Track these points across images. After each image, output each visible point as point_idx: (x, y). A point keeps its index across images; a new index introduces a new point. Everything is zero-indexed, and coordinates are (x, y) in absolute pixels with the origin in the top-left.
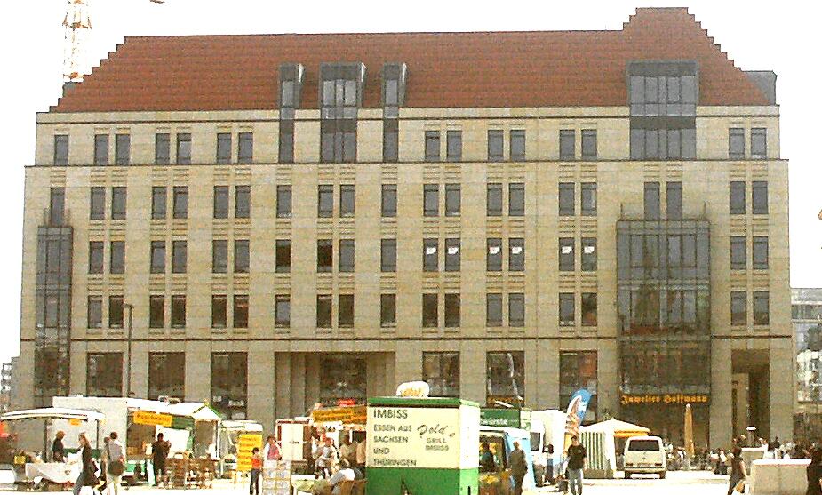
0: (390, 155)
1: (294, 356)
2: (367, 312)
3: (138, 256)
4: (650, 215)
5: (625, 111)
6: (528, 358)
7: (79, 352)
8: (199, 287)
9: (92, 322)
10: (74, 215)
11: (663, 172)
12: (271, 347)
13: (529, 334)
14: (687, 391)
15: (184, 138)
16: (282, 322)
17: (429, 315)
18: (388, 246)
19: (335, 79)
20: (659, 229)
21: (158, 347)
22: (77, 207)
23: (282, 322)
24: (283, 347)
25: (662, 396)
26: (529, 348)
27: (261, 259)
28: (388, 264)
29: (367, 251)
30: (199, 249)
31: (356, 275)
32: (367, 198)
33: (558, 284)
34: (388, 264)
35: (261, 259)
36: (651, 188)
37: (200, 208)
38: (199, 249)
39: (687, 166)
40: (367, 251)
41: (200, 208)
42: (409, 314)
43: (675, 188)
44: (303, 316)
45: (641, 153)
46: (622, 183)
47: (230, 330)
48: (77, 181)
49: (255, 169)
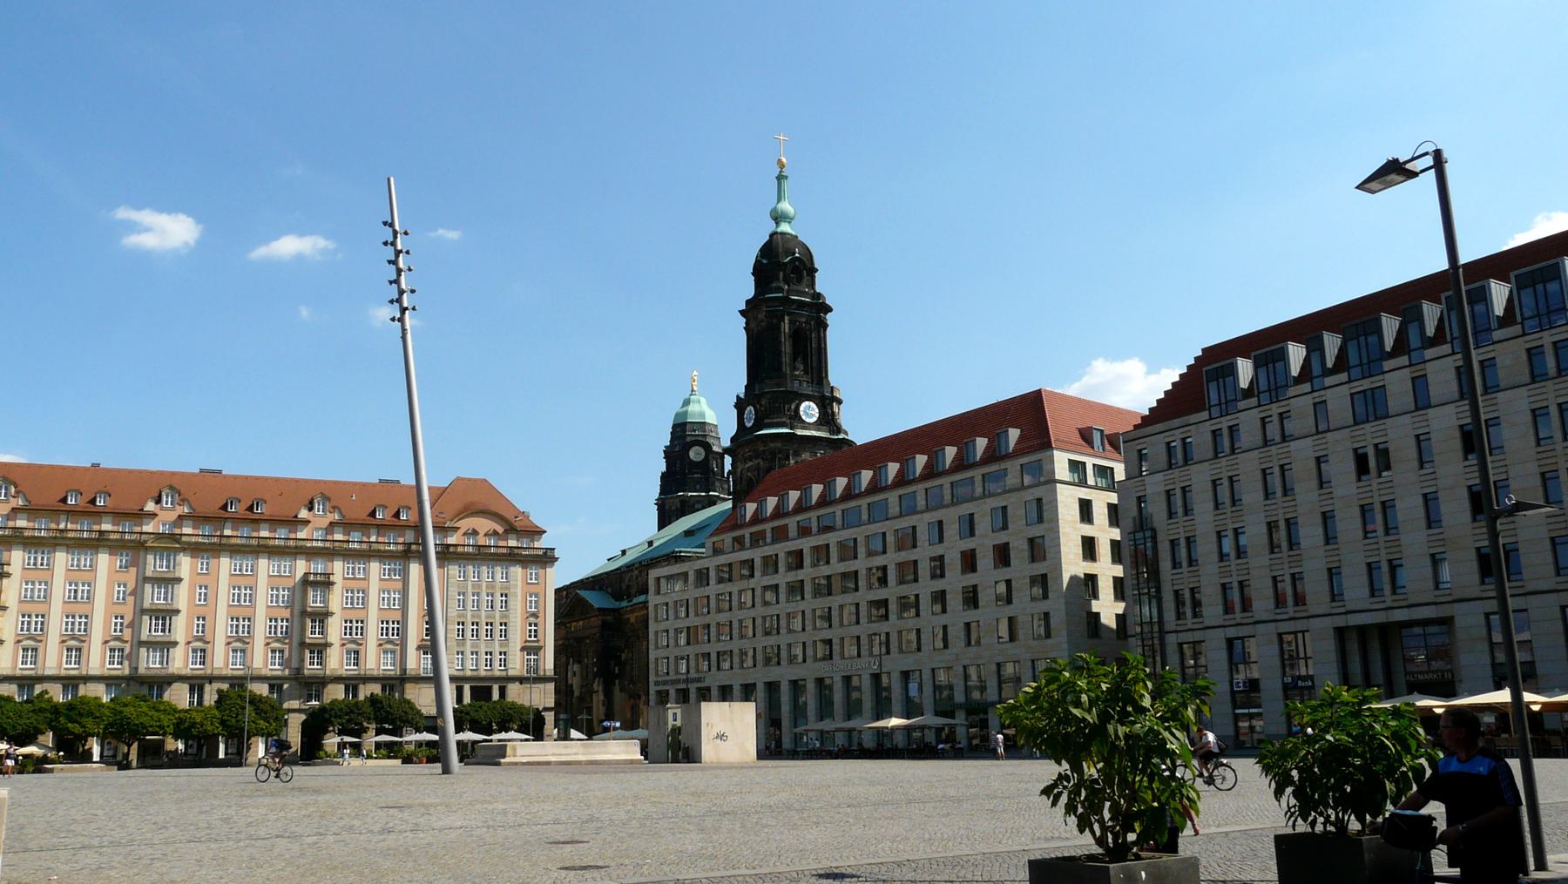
0: (1422, 401)
1: (1362, 630)
2: (1415, 577)
3: (1206, 548)
8: (1260, 569)
9: (1180, 615)
10: (1155, 519)
12: (1329, 623)
15: (1232, 430)
18: (1429, 500)
19: (1357, 338)
22: (1157, 509)
24: (1341, 622)
27: (1310, 534)
28: (1432, 520)
29: (1409, 508)
30: (1255, 534)
31: (1402, 537)
32: (1403, 452)
34: (1432, 520)
35: (1310, 534)
37: (1251, 494)
40: (1409, 508)
41: (1251, 494)
44: (1355, 589)
47: (1291, 609)
48: (1155, 485)
49: (1294, 445)
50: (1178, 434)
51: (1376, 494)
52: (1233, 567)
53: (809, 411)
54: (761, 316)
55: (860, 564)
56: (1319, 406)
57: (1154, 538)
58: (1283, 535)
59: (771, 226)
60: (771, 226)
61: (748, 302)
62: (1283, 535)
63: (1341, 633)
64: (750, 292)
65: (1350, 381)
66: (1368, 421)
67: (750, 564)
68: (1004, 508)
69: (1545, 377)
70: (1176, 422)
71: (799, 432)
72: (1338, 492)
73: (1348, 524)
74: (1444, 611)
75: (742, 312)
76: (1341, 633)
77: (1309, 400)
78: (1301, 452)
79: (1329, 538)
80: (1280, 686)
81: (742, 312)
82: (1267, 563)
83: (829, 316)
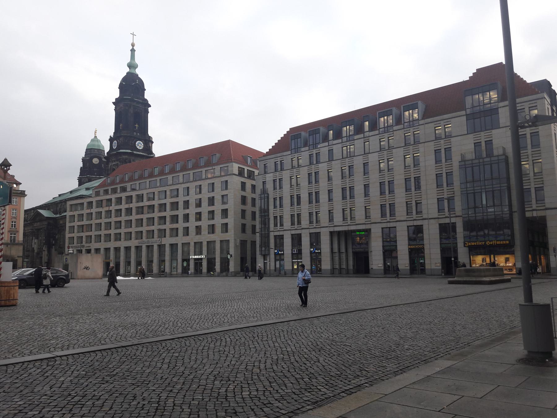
1: (339, 233)
2: (360, 215)
3: (286, 201)
4: (478, 155)
5: (463, 113)
6: (425, 228)
7: (272, 235)
9: (276, 225)
10: (269, 190)
11: (483, 137)
13: (424, 217)
14: (498, 239)
16: (331, 219)
17: (383, 215)
20: (479, 163)
21: (293, 232)
22: (269, 186)
23: (331, 219)
24: (332, 229)
25: (485, 241)
26: (425, 223)
27: (324, 197)
29: (359, 190)
30: (305, 197)
33: (436, 194)
35: (324, 197)
36: (477, 145)
38: (305, 197)
39: (494, 131)
40: (359, 190)
42: (376, 214)
43: (489, 143)
44: (338, 218)
45: (472, 130)
46: (464, 146)
50: (279, 159)
51: (347, 184)
52: (296, 209)
53: (140, 145)
54: (121, 105)
55: (156, 203)
56: (331, 152)
57: (268, 197)
58: (314, 198)
59: (128, 70)
60: (128, 70)
61: (116, 99)
62: (314, 198)
63: (332, 233)
64: (117, 95)
65: (342, 142)
66: (347, 157)
67: (110, 200)
68: (213, 184)
69: (410, 144)
70: (279, 155)
71: (135, 152)
72: (334, 183)
73: (337, 195)
74: (368, 227)
75: (114, 103)
76: (332, 233)
77: (327, 149)
78: (323, 167)
79: (330, 200)
80: (309, 252)
81: (114, 103)
82: (308, 207)
83: (149, 109)
